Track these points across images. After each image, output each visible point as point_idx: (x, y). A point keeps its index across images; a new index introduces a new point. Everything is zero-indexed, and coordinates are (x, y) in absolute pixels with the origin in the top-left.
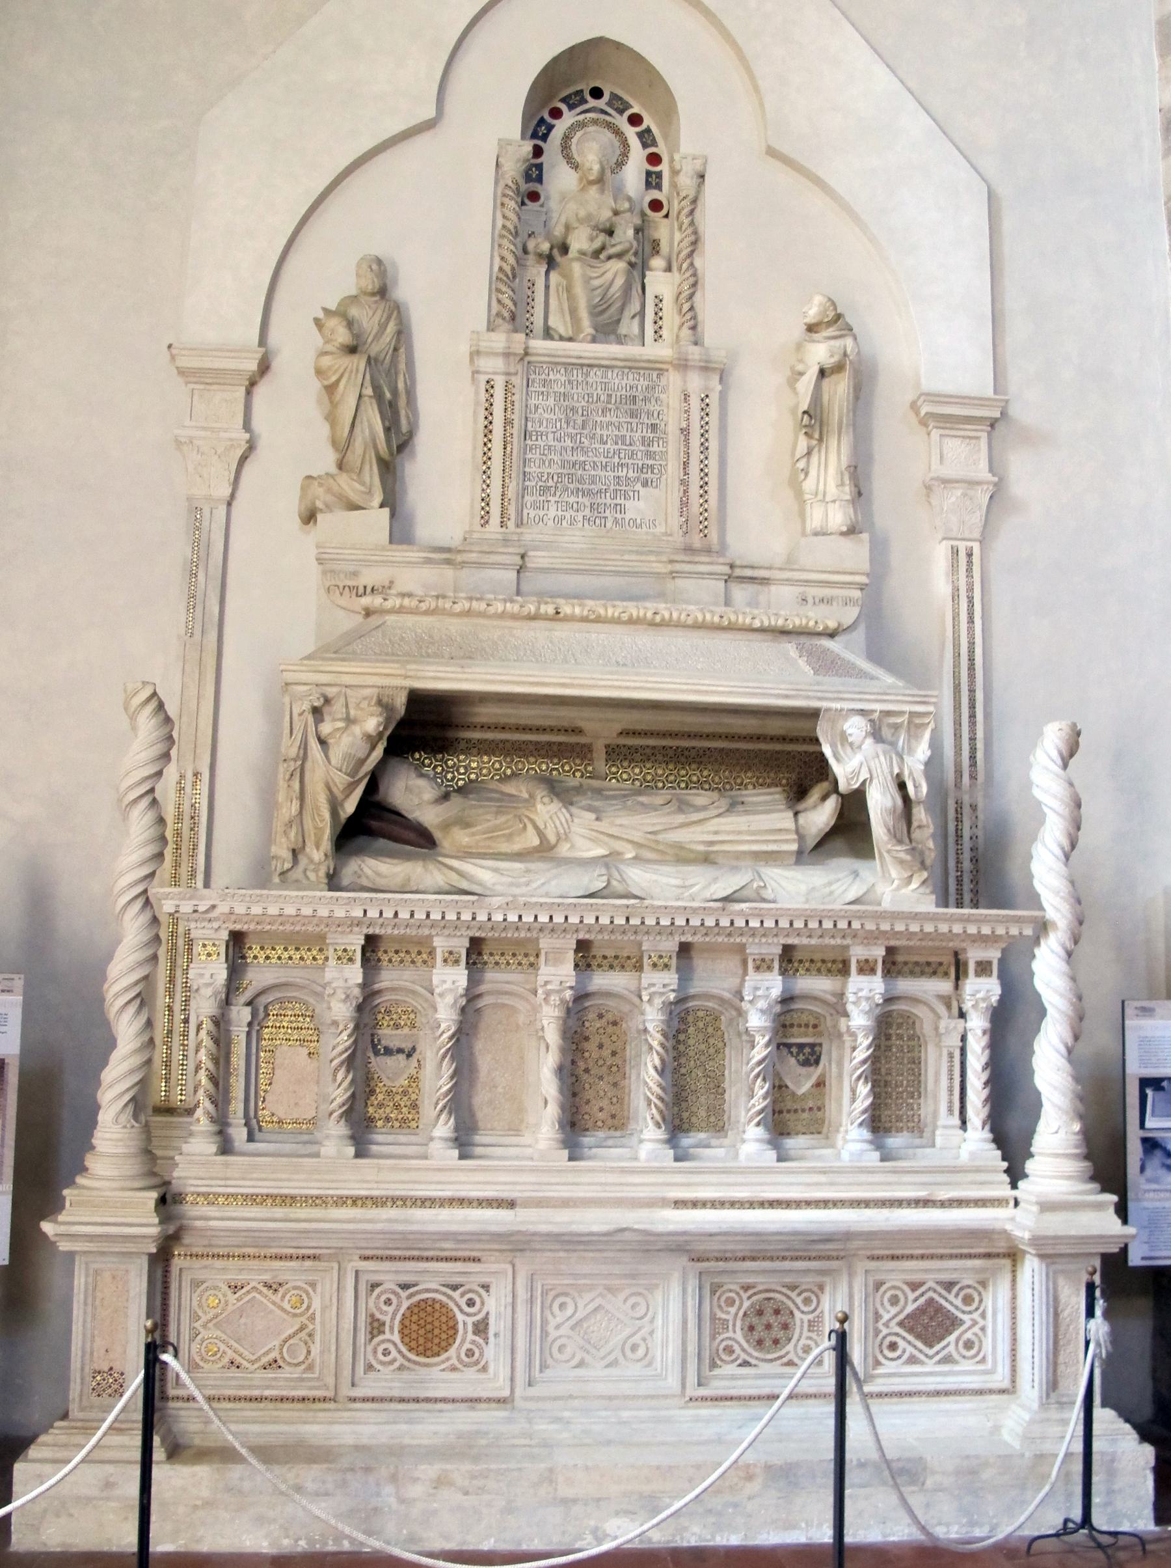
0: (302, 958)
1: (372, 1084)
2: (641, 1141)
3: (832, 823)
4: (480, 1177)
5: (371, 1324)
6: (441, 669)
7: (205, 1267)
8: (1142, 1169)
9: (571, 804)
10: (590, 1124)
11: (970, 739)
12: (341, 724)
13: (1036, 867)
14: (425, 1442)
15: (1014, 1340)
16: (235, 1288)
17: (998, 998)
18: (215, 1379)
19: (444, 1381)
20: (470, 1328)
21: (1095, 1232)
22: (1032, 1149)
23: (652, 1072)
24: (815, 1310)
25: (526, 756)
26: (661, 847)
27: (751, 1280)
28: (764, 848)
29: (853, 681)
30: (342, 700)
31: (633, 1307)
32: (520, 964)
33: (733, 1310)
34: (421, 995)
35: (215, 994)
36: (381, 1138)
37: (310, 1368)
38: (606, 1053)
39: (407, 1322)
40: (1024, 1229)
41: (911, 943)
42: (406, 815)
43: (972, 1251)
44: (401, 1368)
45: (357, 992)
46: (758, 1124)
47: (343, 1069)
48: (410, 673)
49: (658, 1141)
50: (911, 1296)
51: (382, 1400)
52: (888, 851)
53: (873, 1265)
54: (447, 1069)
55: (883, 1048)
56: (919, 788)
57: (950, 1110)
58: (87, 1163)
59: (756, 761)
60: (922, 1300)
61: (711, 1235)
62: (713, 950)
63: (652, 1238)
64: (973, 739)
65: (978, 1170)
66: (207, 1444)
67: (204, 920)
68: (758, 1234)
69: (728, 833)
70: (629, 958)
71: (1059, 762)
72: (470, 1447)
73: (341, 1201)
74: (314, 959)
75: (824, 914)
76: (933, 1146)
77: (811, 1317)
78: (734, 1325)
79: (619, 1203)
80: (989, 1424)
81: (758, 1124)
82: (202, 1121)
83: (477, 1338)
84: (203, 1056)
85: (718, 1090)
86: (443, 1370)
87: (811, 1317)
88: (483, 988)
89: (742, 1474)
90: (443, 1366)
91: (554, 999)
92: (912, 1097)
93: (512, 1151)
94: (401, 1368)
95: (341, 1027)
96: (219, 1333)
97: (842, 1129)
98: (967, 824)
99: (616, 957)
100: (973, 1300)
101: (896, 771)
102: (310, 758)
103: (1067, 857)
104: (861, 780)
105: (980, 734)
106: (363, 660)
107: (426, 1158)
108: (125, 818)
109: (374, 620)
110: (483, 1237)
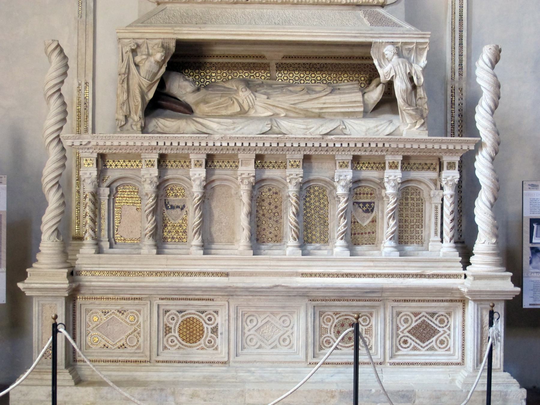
0: (132, 166)
1: (166, 222)
2: (287, 247)
3: (381, 98)
4: (213, 263)
5: (165, 328)
6: (191, 29)
7: (91, 303)
8: (531, 262)
9: (256, 91)
10: (265, 240)
11: (460, 55)
12: (144, 57)
13: (477, 117)
14: (189, 380)
15: (464, 340)
16: (105, 313)
17: (458, 180)
18: (98, 353)
19: (199, 354)
20: (210, 330)
21: (499, 289)
22: (473, 251)
23: (292, 215)
24: (369, 324)
25: (238, 69)
26: (297, 111)
27: (338, 310)
28: (347, 110)
29: (390, 28)
30: (145, 45)
31: (283, 322)
32: (231, 166)
33: (330, 324)
34: (186, 182)
35: (92, 182)
36: (170, 247)
37: (139, 348)
38: (272, 207)
39: (181, 328)
40: (465, 287)
41: (415, 154)
42: (179, 98)
43: (444, 299)
44: (179, 348)
45: (155, 180)
46: (342, 239)
47: (151, 215)
48: (175, 32)
49: (294, 246)
50: (414, 319)
51: (171, 362)
52: (404, 110)
53: (396, 304)
54: (198, 214)
55: (404, 204)
56: (419, 80)
57: (436, 233)
58: (37, 258)
59: (349, 69)
60: (419, 321)
61: (318, 289)
62: (321, 158)
63: (291, 290)
64: (461, 55)
65: (446, 261)
66: (92, 380)
67: (85, 148)
68: (339, 288)
69: (330, 103)
70: (282, 163)
71: (490, 65)
72: (210, 382)
73: (150, 273)
74: (137, 165)
75: (371, 140)
76: (428, 250)
77: (366, 327)
78: (330, 331)
79: (276, 274)
80: (450, 378)
81: (342, 239)
82: (88, 240)
83: (213, 335)
84: (88, 210)
85: (325, 224)
86: (198, 349)
87: (366, 327)
88: (214, 177)
89: (330, 395)
90: (198, 347)
91: (246, 181)
92: (419, 228)
93: (229, 252)
94: (179, 348)
95: (149, 196)
96: (99, 333)
97: (383, 242)
98: (457, 98)
99: (276, 162)
100: (444, 322)
101: (408, 71)
102: (131, 73)
103: (493, 112)
104: (391, 76)
105: (465, 53)
106: (155, 26)
107: (188, 254)
108: (48, 103)
109: (161, 7)
110: (214, 289)
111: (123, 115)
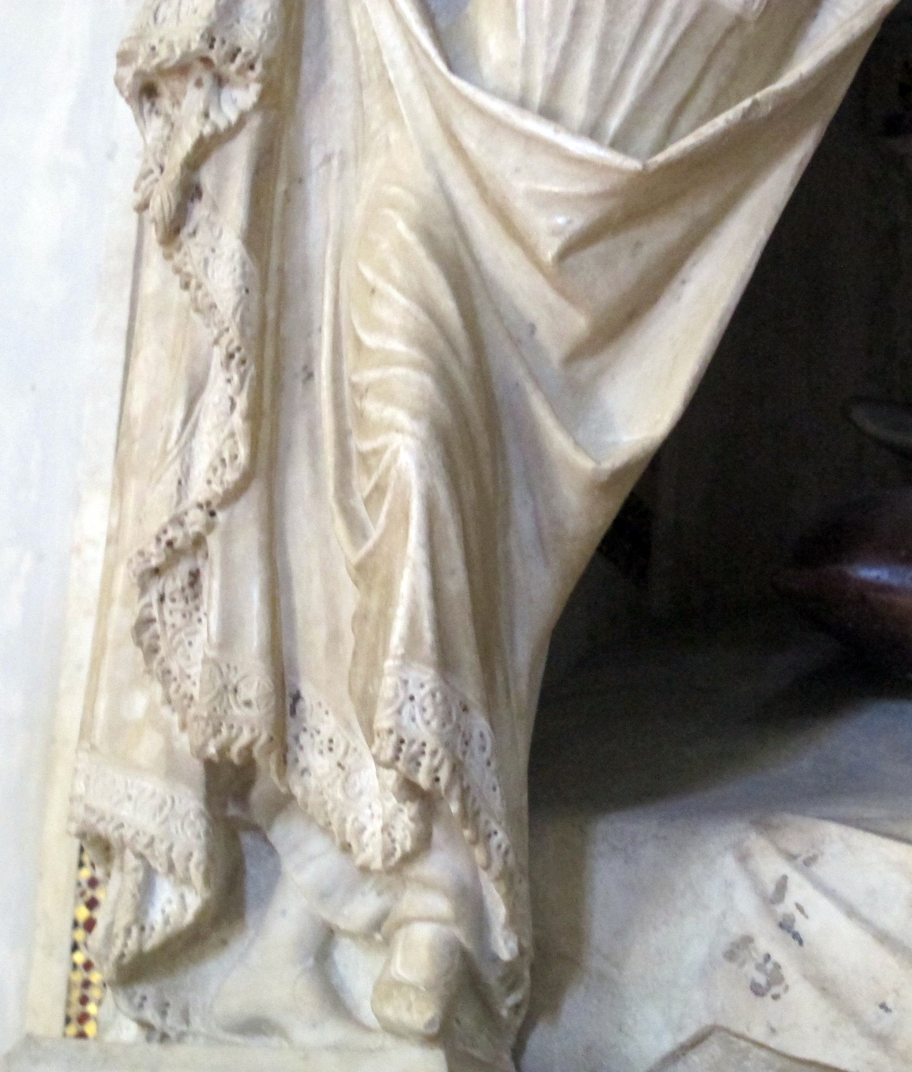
111: (171, 769)
